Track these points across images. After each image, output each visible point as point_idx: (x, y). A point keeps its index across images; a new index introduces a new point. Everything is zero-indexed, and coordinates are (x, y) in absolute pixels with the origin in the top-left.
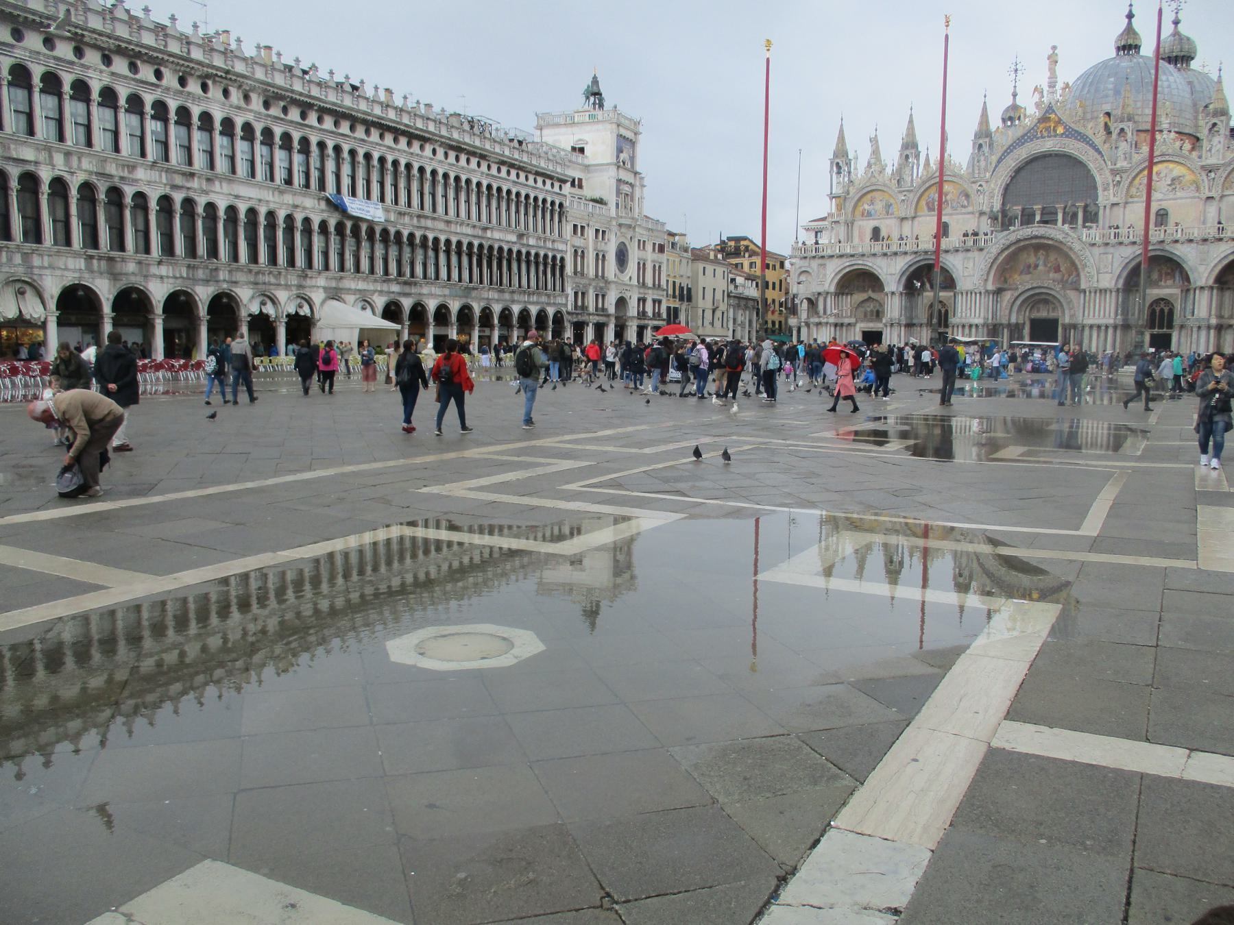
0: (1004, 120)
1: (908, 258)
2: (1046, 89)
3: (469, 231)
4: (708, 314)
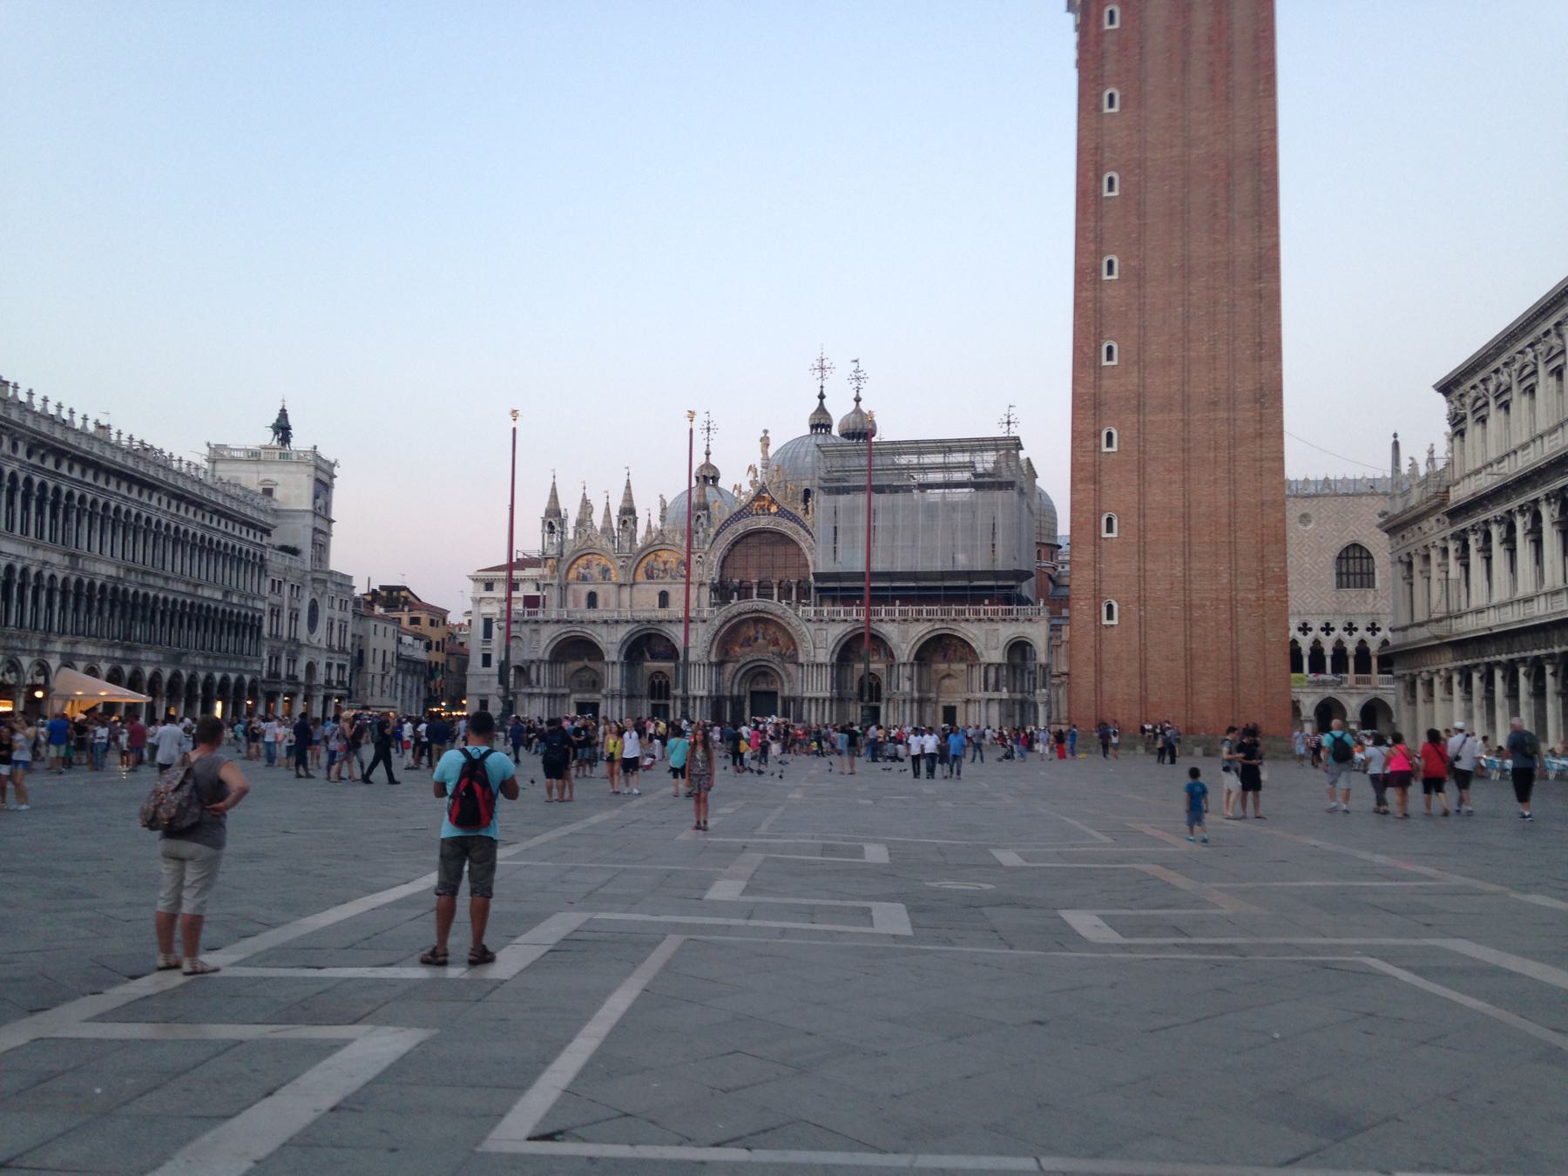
1: (629, 627)
2: (759, 469)
3: (182, 588)
4: (378, 680)
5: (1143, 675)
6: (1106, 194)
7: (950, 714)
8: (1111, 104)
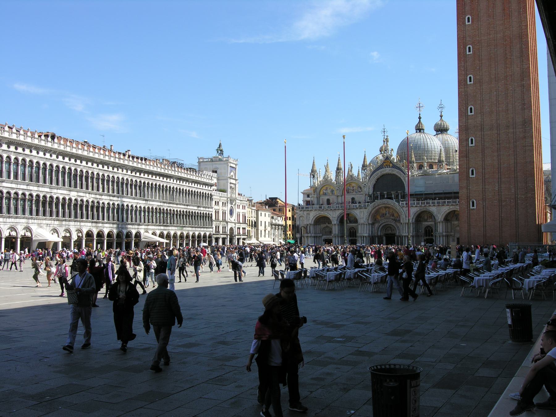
1: (340, 211)
6: (468, 53)
8: (469, 21)
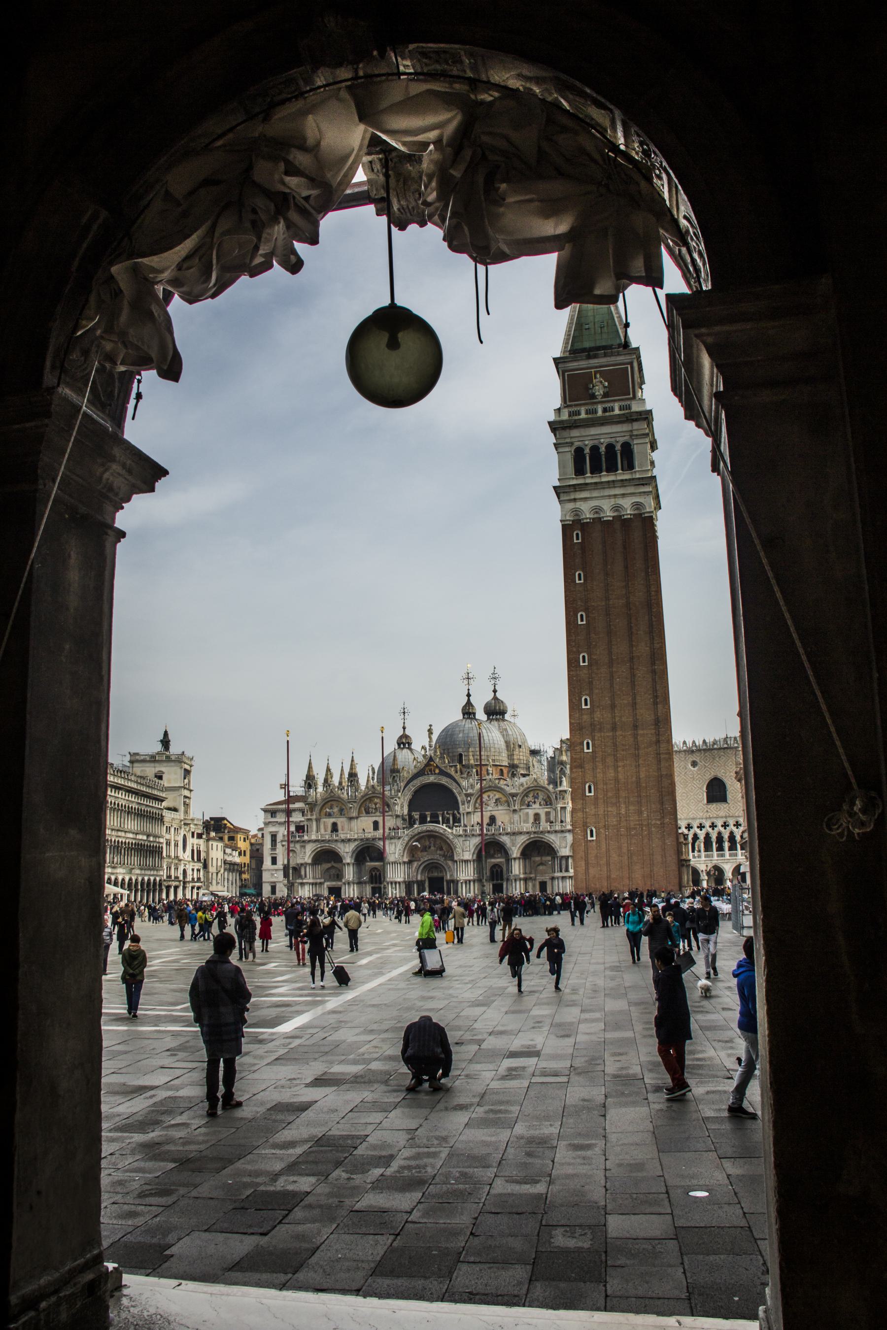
0: (399, 744)
1: (356, 843)
2: (428, 748)
3: (131, 835)
4: (215, 875)
5: (608, 864)
7: (543, 886)
8: (580, 579)
